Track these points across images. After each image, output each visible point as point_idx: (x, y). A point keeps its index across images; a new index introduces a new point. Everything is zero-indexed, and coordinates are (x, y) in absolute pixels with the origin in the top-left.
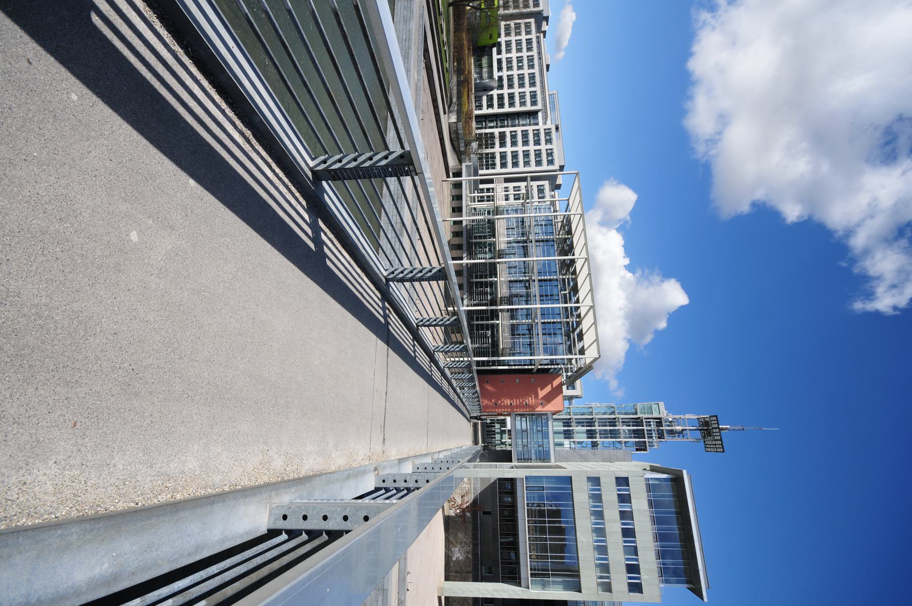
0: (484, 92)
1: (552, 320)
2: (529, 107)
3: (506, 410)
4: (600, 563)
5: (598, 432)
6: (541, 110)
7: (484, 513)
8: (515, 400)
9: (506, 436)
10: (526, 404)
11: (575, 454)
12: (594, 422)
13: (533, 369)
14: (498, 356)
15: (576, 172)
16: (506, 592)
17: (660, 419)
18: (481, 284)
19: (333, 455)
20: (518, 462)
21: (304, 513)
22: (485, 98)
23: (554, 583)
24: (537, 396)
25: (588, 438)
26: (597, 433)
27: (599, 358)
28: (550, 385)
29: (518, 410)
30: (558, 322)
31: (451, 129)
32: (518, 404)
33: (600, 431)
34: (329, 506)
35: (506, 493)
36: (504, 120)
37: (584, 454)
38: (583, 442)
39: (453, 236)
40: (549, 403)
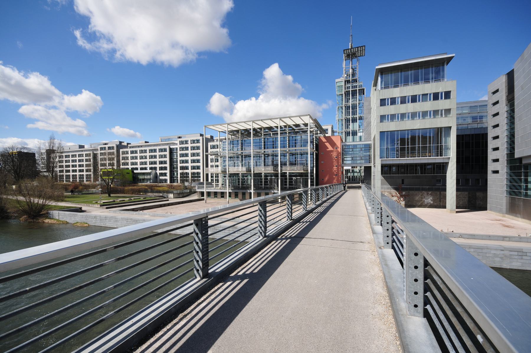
0: (158, 178)
1: (288, 142)
2: (167, 153)
3: (340, 169)
4: (433, 116)
5: (353, 116)
6: (169, 146)
7: (403, 183)
8: (334, 164)
9: (355, 170)
10: (336, 157)
11: (366, 130)
12: (347, 118)
13: (316, 153)
14: (308, 173)
15: (204, 127)
16: (452, 172)
17: (345, 81)
18: (266, 182)
19: (373, 274)
20: (371, 163)
21: (413, 294)
22: (161, 178)
23: (446, 142)
24: (332, 151)
25: (356, 122)
26: (353, 117)
27: (310, 116)
28: (325, 143)
29: (340, 162)
30: (289, 138)
31: (177, 197)
32: (336, 162)
33: (352, 115)
34: (408, 277)
35: (390, 170)
36: (174, 167)
37: (366, 124)
38: (359, 125)
39: (238, 197)
40: (336, 144)
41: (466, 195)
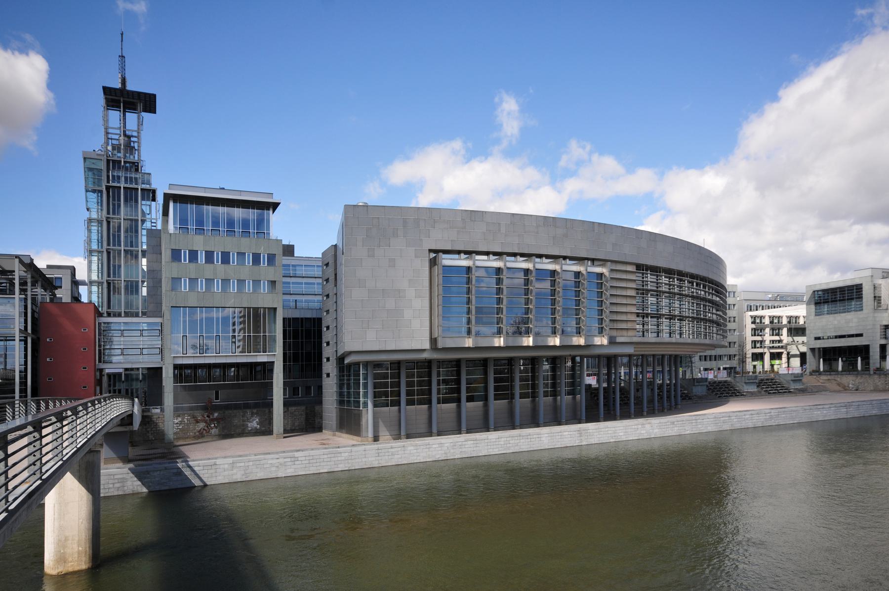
41: (303, 411)
